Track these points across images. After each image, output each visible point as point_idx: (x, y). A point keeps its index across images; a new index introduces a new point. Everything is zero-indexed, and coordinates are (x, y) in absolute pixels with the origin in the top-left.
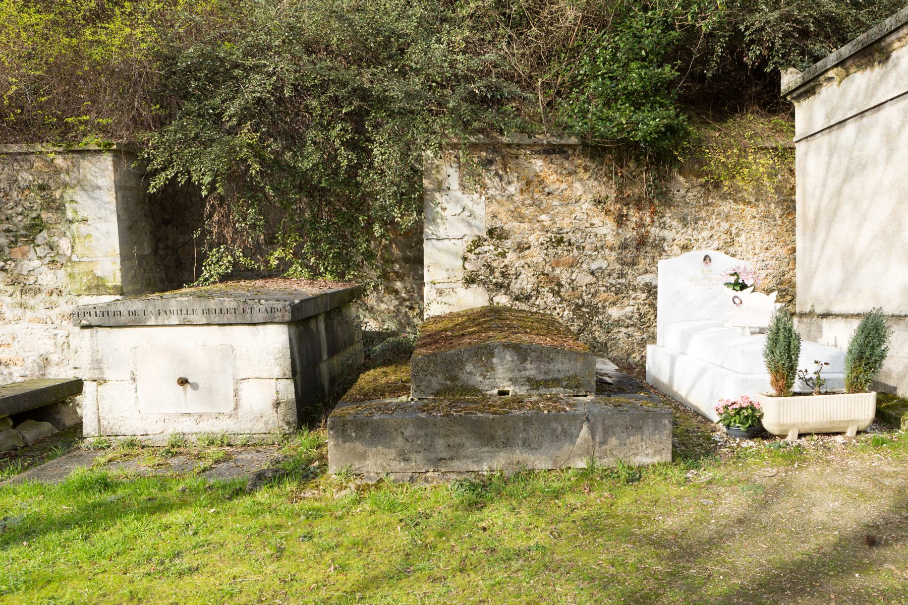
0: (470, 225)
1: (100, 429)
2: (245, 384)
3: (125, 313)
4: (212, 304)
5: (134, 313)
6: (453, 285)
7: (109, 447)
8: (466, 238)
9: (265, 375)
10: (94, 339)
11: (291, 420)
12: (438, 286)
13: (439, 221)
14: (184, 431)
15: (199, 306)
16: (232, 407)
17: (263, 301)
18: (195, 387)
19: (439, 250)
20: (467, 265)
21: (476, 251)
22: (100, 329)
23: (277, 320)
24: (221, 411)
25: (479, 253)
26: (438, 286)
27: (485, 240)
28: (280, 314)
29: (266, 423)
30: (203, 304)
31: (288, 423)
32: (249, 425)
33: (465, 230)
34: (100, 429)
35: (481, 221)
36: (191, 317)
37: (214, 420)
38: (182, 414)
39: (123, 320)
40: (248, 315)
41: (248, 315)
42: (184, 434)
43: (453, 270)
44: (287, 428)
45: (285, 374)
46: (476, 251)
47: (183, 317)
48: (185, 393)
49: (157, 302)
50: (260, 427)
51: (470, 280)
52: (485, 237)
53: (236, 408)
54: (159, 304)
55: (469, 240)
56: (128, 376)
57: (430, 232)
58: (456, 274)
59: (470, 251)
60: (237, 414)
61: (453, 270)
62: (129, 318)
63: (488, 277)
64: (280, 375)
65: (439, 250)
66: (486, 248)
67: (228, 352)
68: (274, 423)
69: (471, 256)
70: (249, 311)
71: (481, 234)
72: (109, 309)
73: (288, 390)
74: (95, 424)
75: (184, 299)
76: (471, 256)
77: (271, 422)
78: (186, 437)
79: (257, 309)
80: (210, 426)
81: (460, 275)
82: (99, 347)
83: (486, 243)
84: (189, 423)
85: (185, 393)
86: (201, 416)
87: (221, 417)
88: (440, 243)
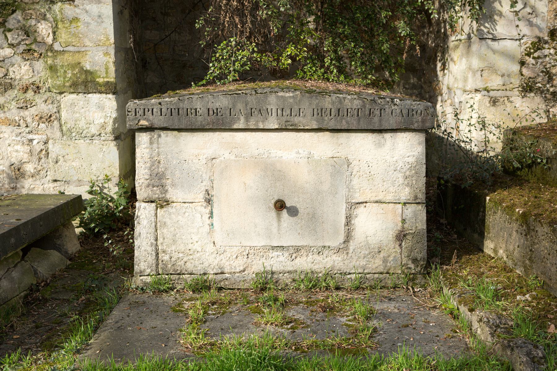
0: (531, 24)
1: (157, 265)
2: (361, 209)
3: (202, 110)
4: (327, 102)
5: (216, 112)
6: (508, 93)
7: (172, 289)
8: (525, 40)
9: (389, 198)
10: (155, 146)
11: (419, 256)
12: (492, 93)
13: (496, 17)
14: (274, 269)
15: (307, 105)
16: (342, 238)
17: (397, 101)
18: (293, 212)
19: (494, 51)
20: (525, 71)
21: (536, 55)
22: (163, 134)
23: (416, 126)
24: (327, 244)
25: (539, 57)
26: (492, 93)
27: (546, 42)
28: (420, 119)
29: (385, 261)
30: (315, 102)
31: (415, 261)
32: (363, 263)
33: (525, 30)
34: (157, 265)
35: (543, 20)
36: (296, 120)
37: (316, 256)
38: (273, 248)
39: (200, 120)
40: (376, 119)
41: (376, 119)
42: (273, 273)
43: (509, 76)
44: (412, 266)
45: (416, 197)
46: (536, 55)
47: (284, 119)
48: (279, 220)
49: (249, 98)
50: (376, 264)
51: (528, 88)
52: (546, 38)
53: (347, 241)
54: (252, 100)
55: (528, 42)
56: (201, 197)
57: (485, 30)
58: (513, 80)
59: (529, 55)
60: (346, 249)
61: (509, 76)
62: (209, 118)
63: (545, 86)
64: (410, 198)
65: (494, 51)
66: (546, 52)
67: (341, 167)
68: (395, 259)
69: (530, 60)
70: (378, 113)
71: (541, 35)
72: (181, 105)
73: (417, 217)
74: (151, 259)
75: (287, 95)
76: (530, 60)
77: (391, 259)
78: (275, 276)
79: (388, 111)
80: (305, 263)
81: (516, 81)
82: (162, 157)
83: (546, 46)
84: (281, 258)
85: (279, 220)
86: (298, 249)
87: (326, 252)
88: (496, 43)
